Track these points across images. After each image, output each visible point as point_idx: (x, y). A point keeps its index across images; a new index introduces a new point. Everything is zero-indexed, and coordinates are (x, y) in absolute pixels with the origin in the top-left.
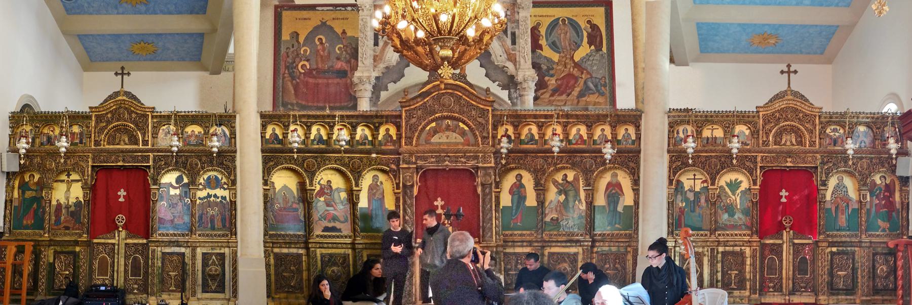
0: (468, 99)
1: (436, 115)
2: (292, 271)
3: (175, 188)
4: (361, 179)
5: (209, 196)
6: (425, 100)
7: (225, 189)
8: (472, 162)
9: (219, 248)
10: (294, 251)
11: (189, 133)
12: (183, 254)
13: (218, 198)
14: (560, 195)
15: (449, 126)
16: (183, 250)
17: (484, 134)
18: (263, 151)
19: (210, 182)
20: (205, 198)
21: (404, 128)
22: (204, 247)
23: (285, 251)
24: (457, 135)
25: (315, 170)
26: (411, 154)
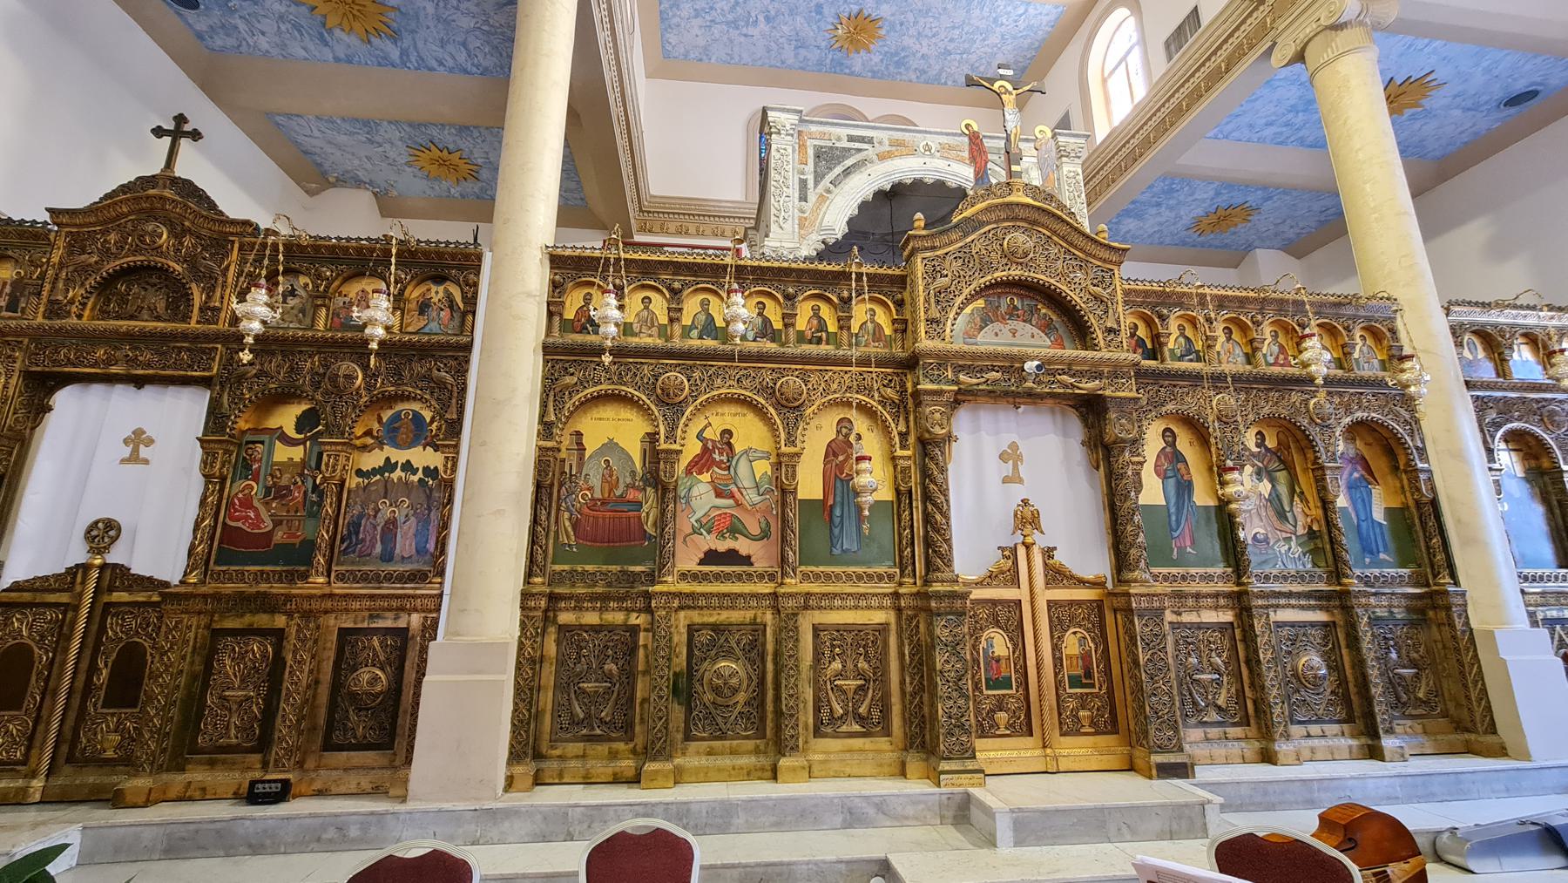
0: (1065, 245)
1: (996, 275)
2: (608, 677)
3: (292, 443)
4: (802, 425)
5: (389, 466)
6: (969, 239)
7: (436, 448)
8: (1089, 385)
9: (391, 615)
10: (617, 617)
11: (352, 295)
12: (279, 635)
13: (414, 472)
14: (1260, 480)
15: (1015, 308)
16: (280, 621)
17: (1109, 325)
18: (548, 349)
19: (395, 430)
20: (374, 472)
21: (922, 299)
22: (347, 610)
23: (591, 618)
24: (1036, 331)
25: (685, 400)
26: (943, 359)
